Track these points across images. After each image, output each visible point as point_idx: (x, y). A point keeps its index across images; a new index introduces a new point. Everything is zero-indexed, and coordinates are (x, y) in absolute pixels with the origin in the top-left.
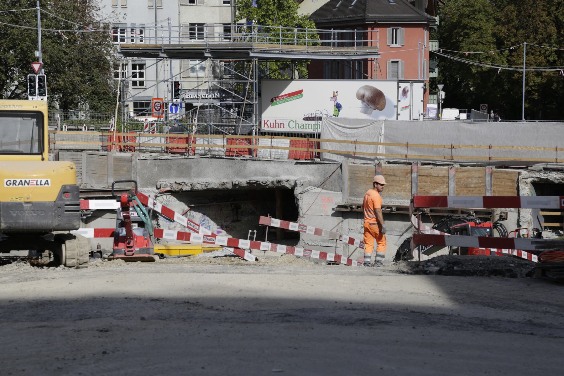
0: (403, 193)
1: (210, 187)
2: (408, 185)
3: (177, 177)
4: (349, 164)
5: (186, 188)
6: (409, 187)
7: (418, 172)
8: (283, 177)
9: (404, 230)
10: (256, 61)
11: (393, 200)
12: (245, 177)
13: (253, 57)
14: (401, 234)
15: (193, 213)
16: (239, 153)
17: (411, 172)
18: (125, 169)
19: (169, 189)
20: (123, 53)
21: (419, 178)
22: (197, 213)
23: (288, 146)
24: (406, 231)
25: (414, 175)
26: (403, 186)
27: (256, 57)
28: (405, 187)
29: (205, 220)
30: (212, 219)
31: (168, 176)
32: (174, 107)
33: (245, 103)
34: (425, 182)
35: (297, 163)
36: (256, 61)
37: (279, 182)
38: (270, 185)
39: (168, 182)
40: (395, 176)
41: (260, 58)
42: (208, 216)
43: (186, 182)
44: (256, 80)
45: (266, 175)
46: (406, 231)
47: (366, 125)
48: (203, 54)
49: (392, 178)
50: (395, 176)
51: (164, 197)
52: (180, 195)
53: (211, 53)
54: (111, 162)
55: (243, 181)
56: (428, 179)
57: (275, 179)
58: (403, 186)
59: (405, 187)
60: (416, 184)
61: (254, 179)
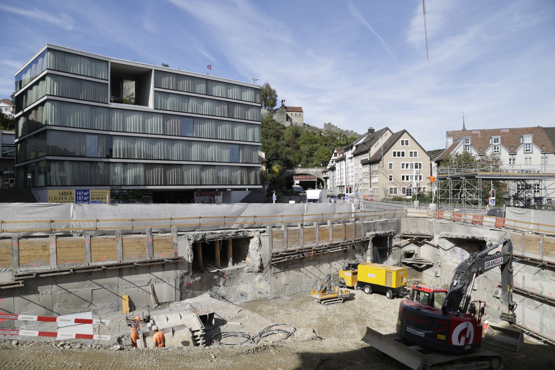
0: (536, 251)
1: (458, 237)
2: (538, 247)
3: (448, 231)
4: (510, 232)
5: (449, 237)
6: (538, 248)
7: (543, 240)
8: (485, 236)
9: (536, 272)
10: (480, 180)
11: (531, 254)
12: (471, 234)
13: (478, 178)
14: (534, 274)
15: (456, 247)
16: (476, 222)
17: (539, 240)
18: (431, 226)
19: (443, 236)
20: (438, 179)
21: (544, 244)
22: (459, 248)
23: (495, 221)
24: (537, 273)
25: (541, 242)
26: (536, 247)
27: (480, 178)
28: (537, 248)
29: (463, 251)
30: (466, 251)
31: (444, 231)
32: (492, 201)
33: (452, 199)
34: (547, 246)
35: (491, 229)
36: (480, 180)
37: (483, 238)
38: (480, 239)
39: (444, 233)
40: (531, 241)
41: (482, 178)
42: (465, 249)
43: (450, 234)
44: (480, 188)
45: (479, 234)
46: (537, 273)
47: (525, 212)
48: (460, 177)
49: (531, 242)
50: (531, 241)
51: (442, 239)
52: (451, 240)
53: (464, 177)
54: (427, 223)
55: (470, 236)
56: (548, 245)
57: (482, 236)
58: (536, 247)
59: (537, 248)
60: (542, 247)
61: (474, 235)
